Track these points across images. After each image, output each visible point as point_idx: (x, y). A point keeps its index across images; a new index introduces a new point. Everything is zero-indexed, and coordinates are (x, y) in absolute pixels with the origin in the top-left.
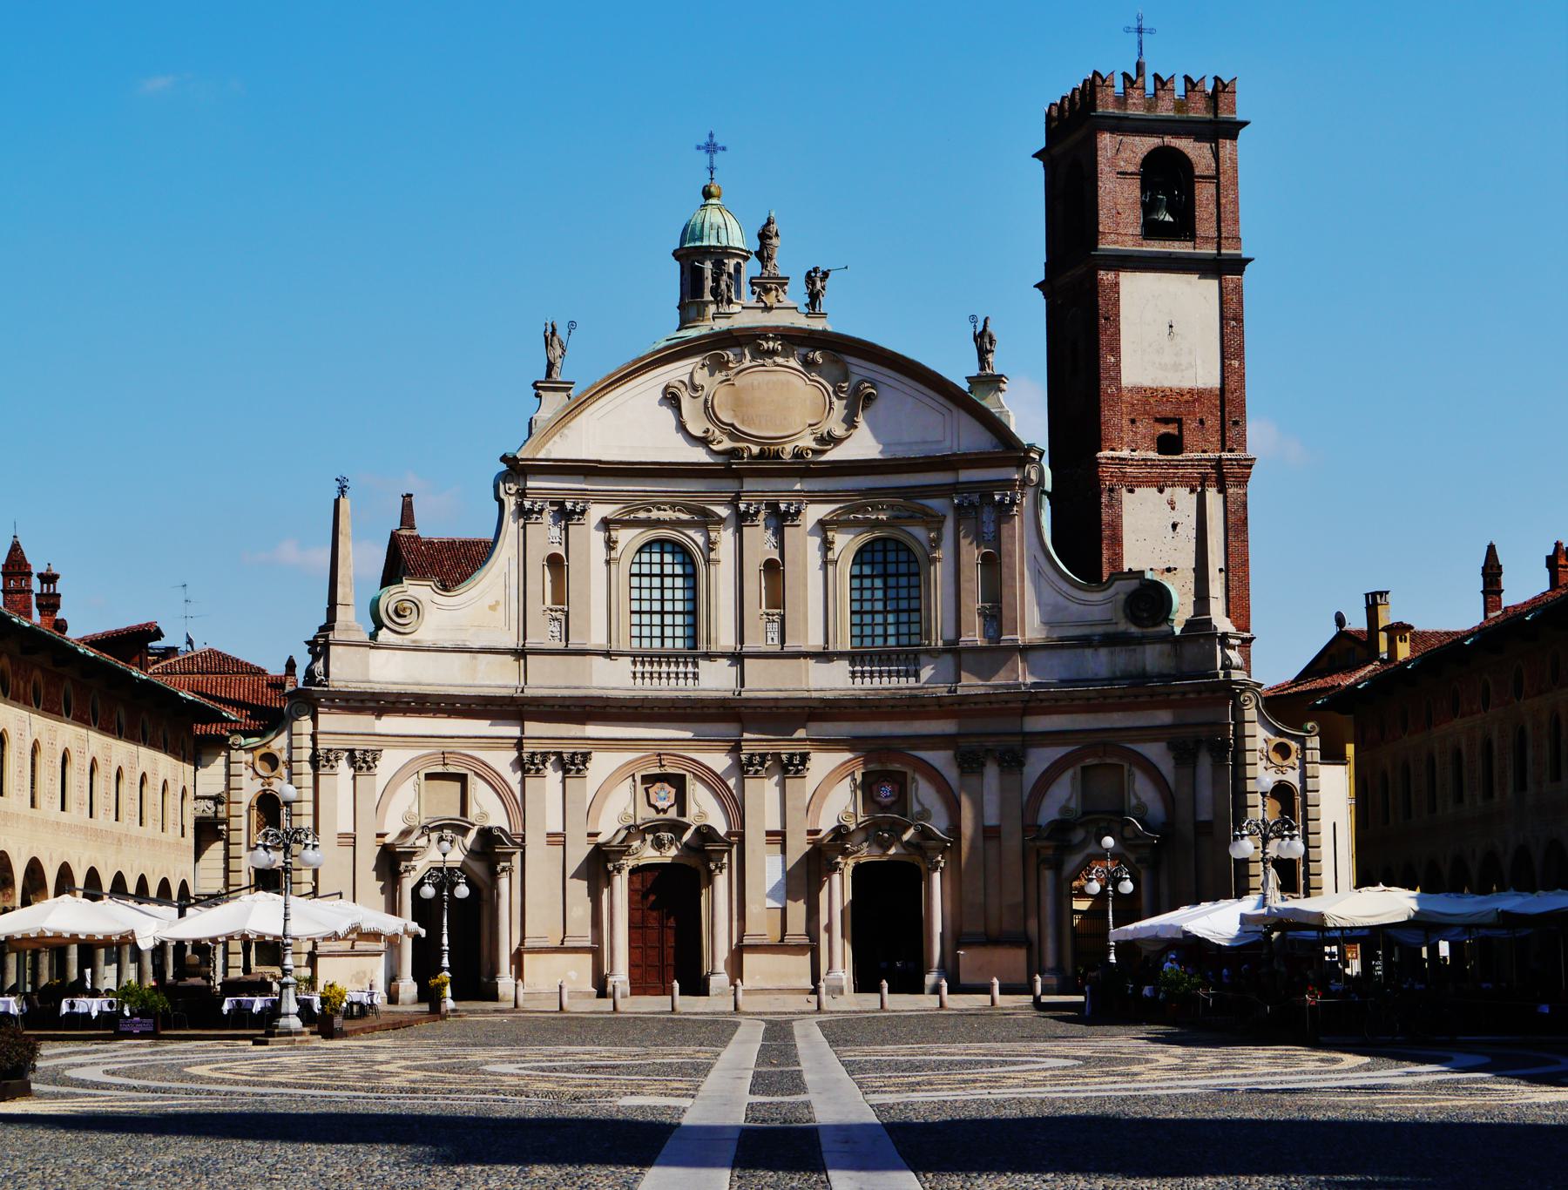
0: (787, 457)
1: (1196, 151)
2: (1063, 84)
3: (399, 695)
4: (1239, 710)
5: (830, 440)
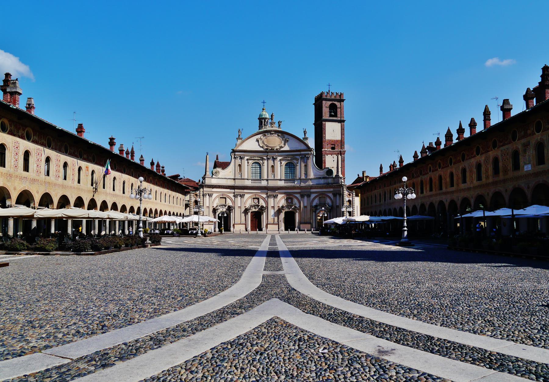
0: (275, 150)
1: (338, 104)
2: (318, 93)
3: (216, 185)
4: (343, 189)
5: (281, 147)
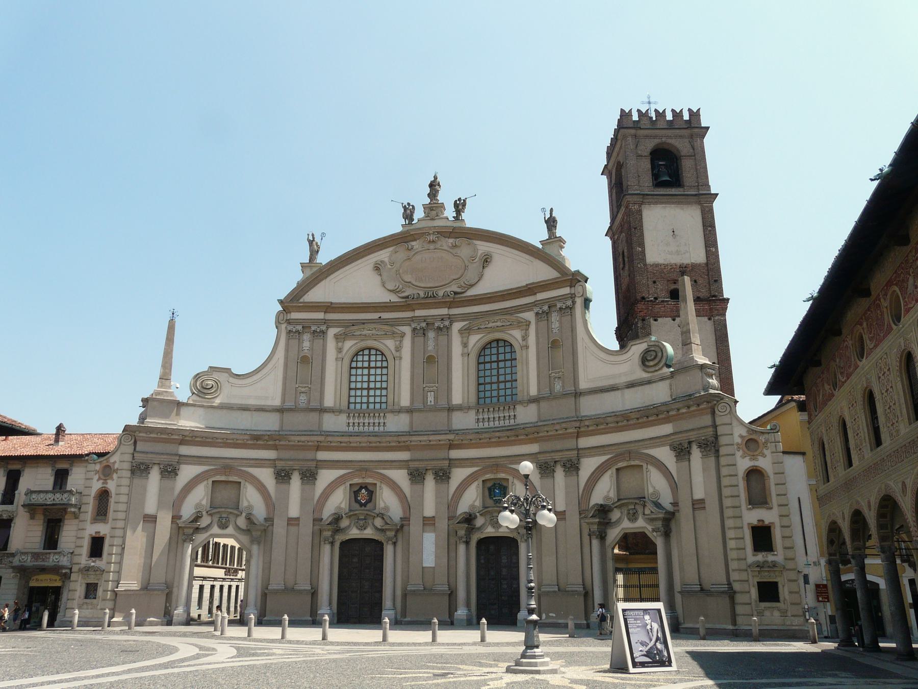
1: (681, 145)
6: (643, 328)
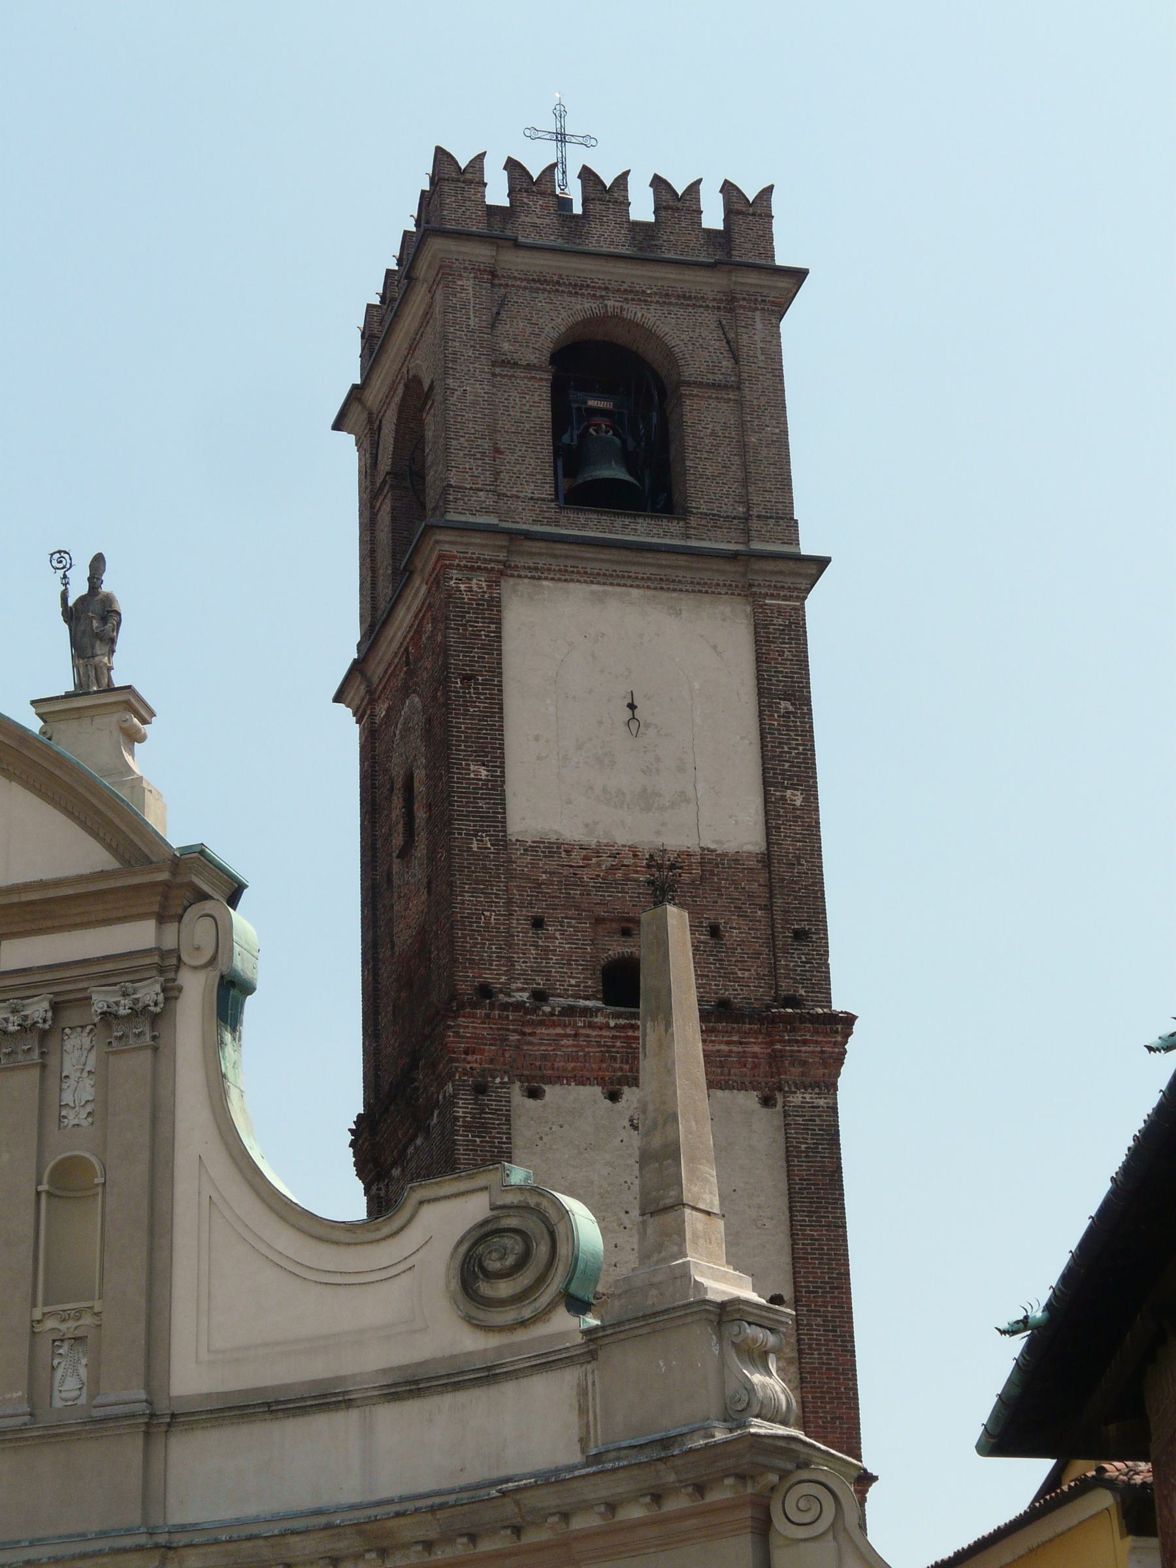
6: (479, 1126)
